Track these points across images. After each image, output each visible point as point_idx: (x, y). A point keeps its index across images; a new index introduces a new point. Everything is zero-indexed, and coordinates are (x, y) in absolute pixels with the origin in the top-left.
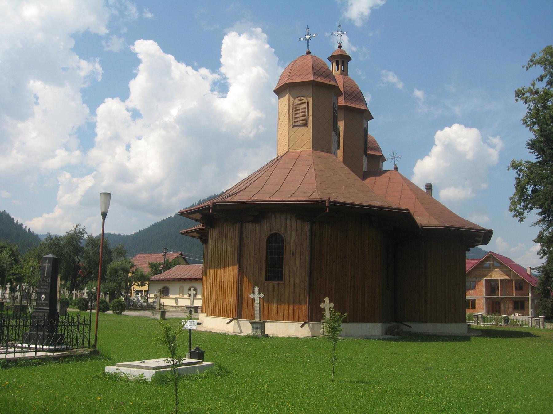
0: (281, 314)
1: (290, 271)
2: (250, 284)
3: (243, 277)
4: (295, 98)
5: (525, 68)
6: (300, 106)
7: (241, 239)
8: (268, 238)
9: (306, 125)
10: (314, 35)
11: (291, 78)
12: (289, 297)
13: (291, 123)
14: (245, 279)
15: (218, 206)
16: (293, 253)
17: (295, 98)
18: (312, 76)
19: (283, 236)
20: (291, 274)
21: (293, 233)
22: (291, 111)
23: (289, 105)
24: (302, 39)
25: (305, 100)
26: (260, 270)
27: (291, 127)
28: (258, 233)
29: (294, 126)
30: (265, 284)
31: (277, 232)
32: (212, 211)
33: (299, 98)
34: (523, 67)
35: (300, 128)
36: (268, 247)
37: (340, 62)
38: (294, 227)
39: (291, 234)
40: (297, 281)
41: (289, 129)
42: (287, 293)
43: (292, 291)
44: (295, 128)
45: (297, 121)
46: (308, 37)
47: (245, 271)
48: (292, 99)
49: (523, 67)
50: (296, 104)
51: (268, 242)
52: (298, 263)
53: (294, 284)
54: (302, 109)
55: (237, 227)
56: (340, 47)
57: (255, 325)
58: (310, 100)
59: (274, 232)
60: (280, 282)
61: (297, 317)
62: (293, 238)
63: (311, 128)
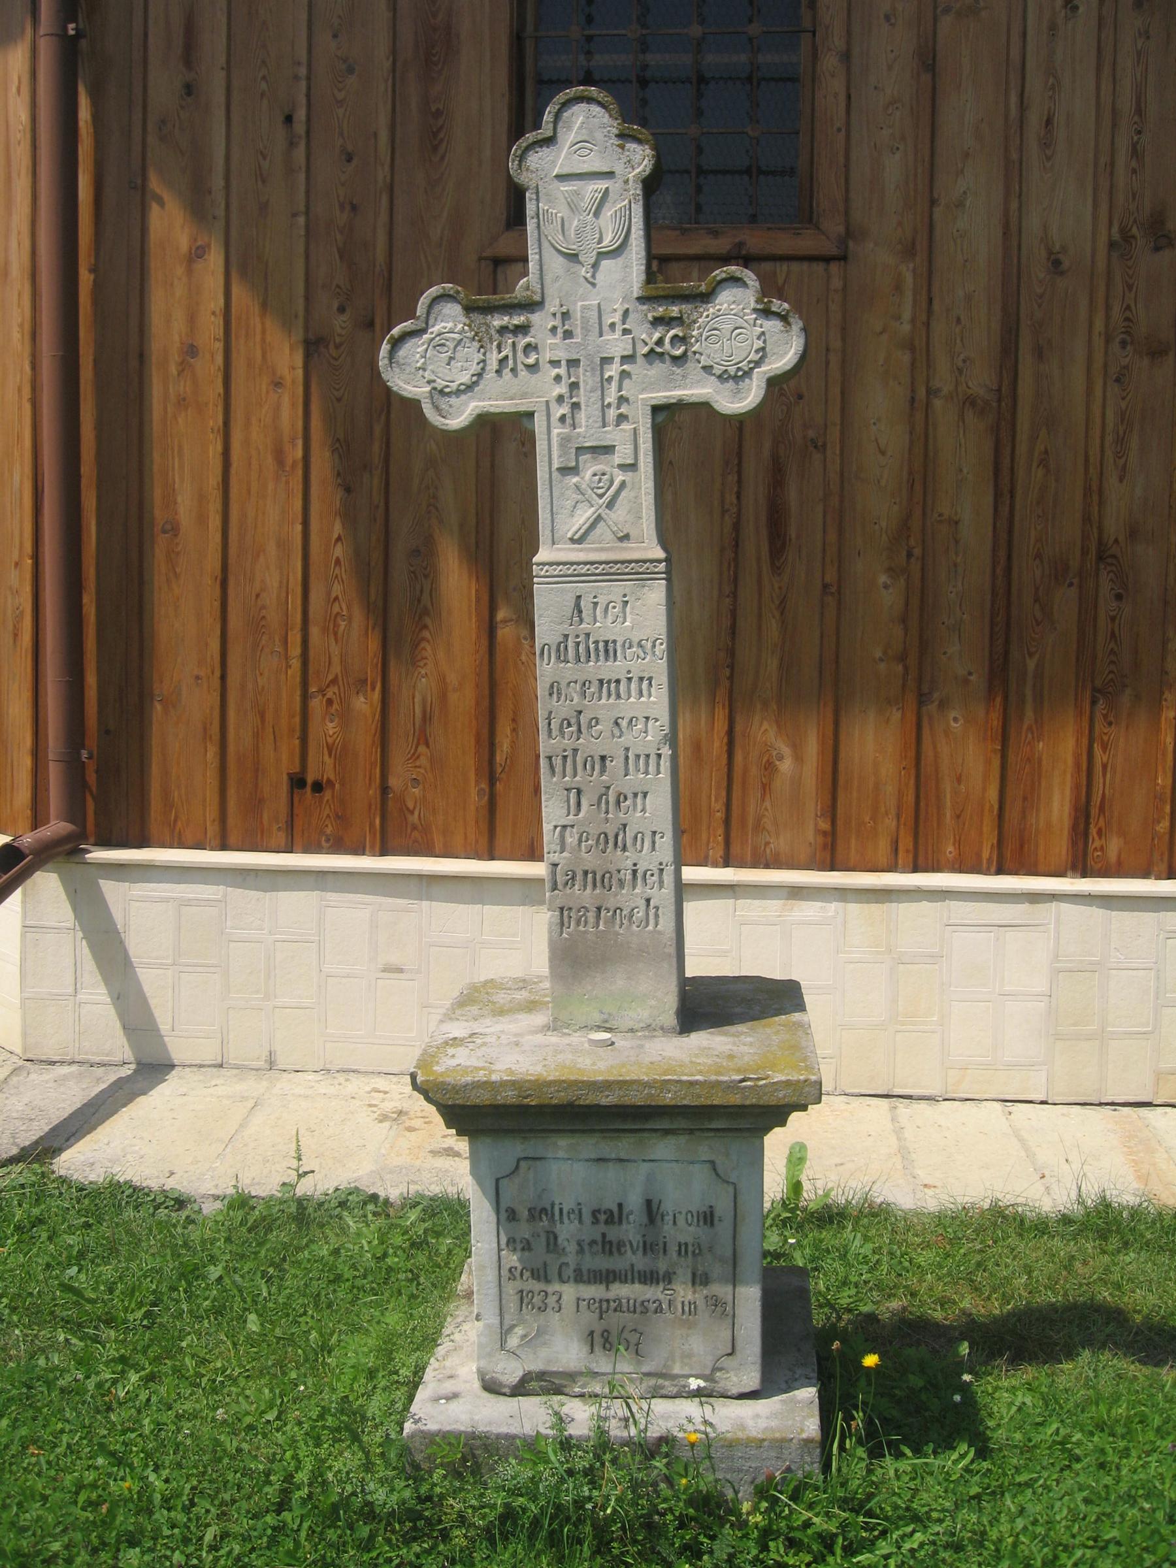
1: (928, 61)
3: (141, 196)
12: (921, 475)
14: (169, 224)
20: (967, 110)
40: (1067, 210)
43: (980, 380)
47: (163, 86)
61: (1057, 807)
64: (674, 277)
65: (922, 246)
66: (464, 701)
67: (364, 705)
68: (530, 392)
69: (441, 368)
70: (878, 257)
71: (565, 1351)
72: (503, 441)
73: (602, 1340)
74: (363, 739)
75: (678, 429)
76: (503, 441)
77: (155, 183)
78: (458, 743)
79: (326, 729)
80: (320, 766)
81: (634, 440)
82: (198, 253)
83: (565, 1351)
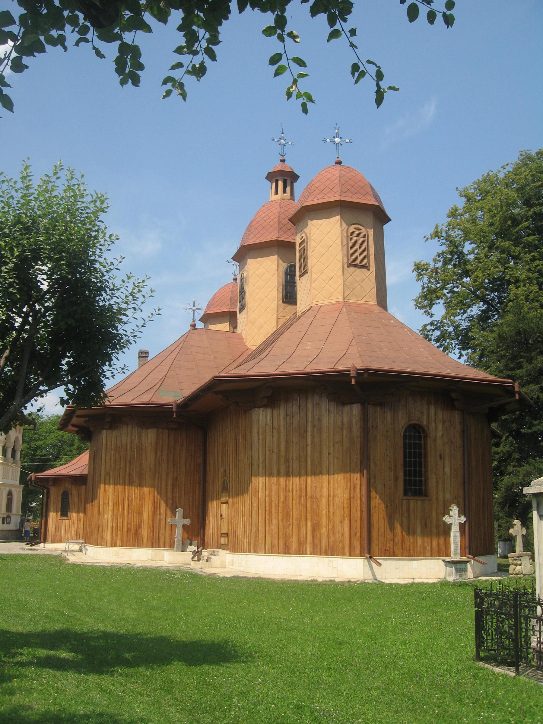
0: (428, 548)
1: (437, 482)
2: (381, 502)
4: (349, 225)
5: (425, 238)
6: (358, 238)
7: (366, 429)
8: (405, 431)
9: (367, 267)
10: (347, 141)
11: (344, 195)
13: (345, 260)
14: (373, 494)
15: (366, 375)
16: (440, 456)
17: (349, 225)
18: (374, 199)
19: (426, 429)
20: (440, 486)
21: (440, 426)
22: (345, 243)
23: (342, 233)
24: (328, 140)
25: (363, 230)
26: (396, 479)
27: (346, 266)
28: (391, 423)
29: (350, 265)
30: (404, 502)
31: (417, 422)
32: (356, 382)
33: (356, 226)
34: (425, 237)
35: (358, 270)
36: (405, 444)
37: (289, 182)
38: (440, 417)
39: (436, 428)
41: (343, 267)
42: (434, 514)
44: (352, 269)
45: (354, 259)
46: (337, 140)
48: (345, 226)
49: (425, 237)
50: (353, 234)
51: (405, 436)
52: (447, 470)
53: (444, 501)
54: (361, 243)
55: (356, 409)
56: (283, 161)
57: (458, 566)
58: (371, 232)
59: (414, 422)
60: (424, 498)
62: (440, 434)
63: (374, 275)
64: (459, 516)
65: (437, 499)
66: (400, 542)
67: (392, 542)
68: (453, 522)
69: (446, 519)
70: (434, 499)
71: (458, 577)
72: (451, 524)
73: (460, 577)
74: (392, 546)
75: (460, 523)
76: (451, 524)
77: (372, 489)
78: (400, 546)
79: (388, 545)
80: (388, 548)
81: (458, 524)
82: (376, 497)
83: (458, 577)
